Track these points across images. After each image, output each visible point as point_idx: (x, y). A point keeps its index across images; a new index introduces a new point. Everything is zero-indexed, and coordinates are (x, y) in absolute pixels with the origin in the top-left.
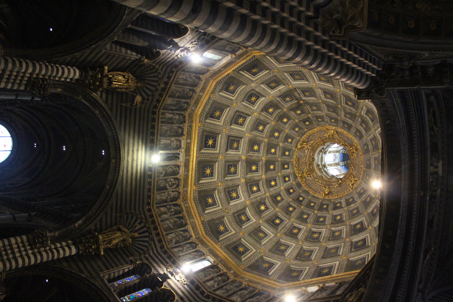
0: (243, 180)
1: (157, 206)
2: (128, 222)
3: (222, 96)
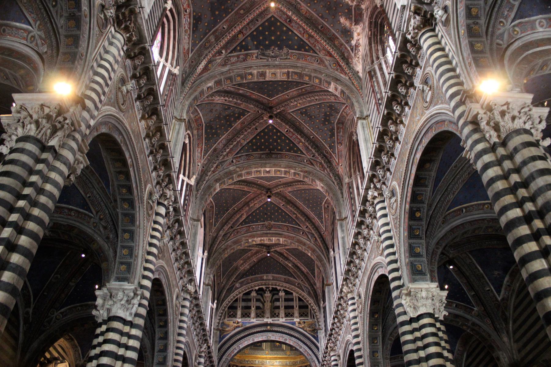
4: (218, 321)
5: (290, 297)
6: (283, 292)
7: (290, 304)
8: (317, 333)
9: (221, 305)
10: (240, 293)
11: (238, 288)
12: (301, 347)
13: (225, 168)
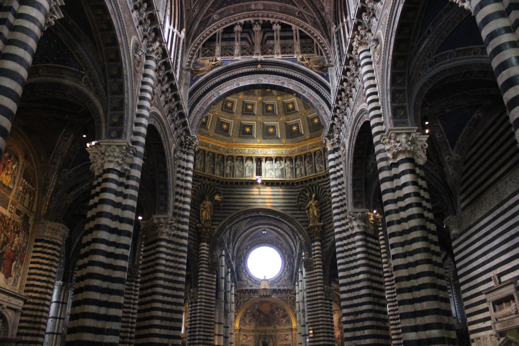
0: (279, 98)
1: (295, 177)
2: (305, 200)
3: (211, 126)
5: (288, 34)
8: (327, 71)
9: (192, 41)
10: (218, 27)
11: (216, 21)
12: (304, 92)
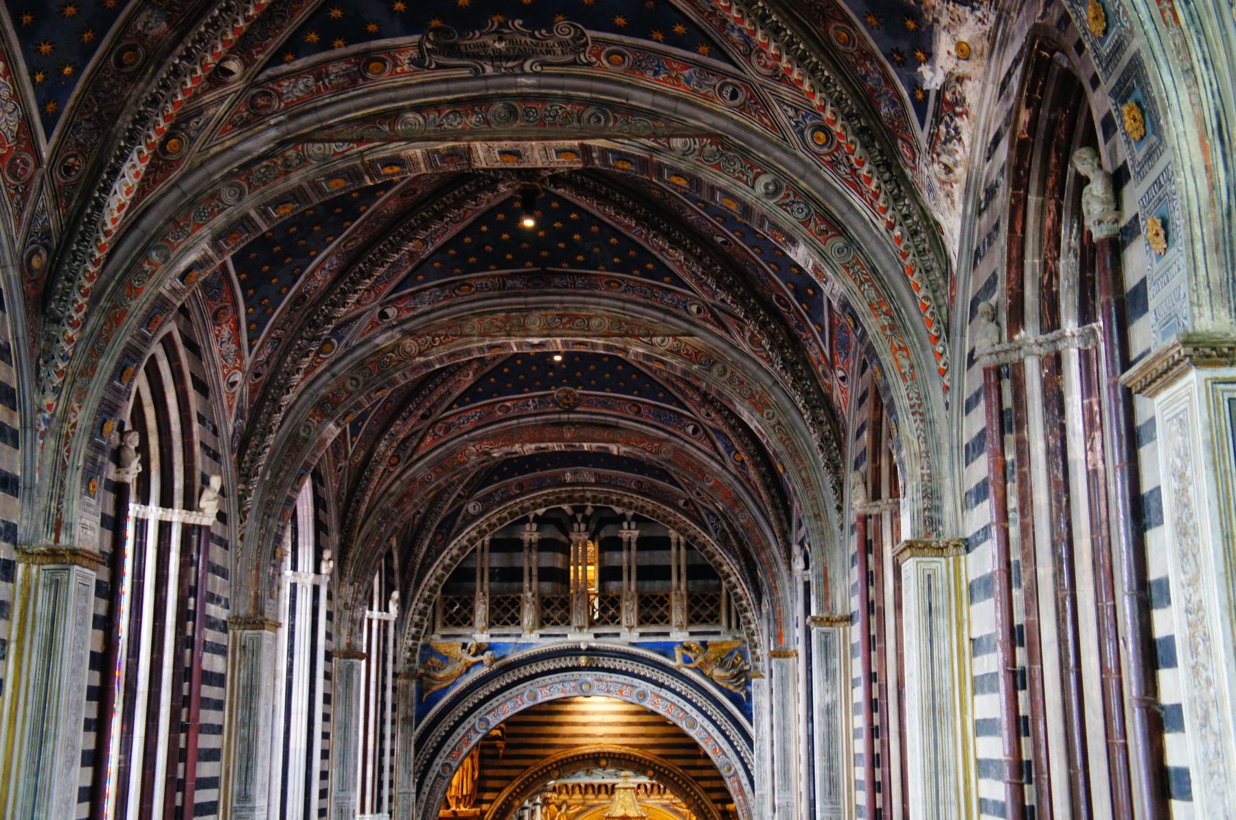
4: (410, 642)
6: (633, 525)
7: (656, 558)
8: (748, 683)
9: (418, 584)
10: (482, 533)
13: (354, 343)
